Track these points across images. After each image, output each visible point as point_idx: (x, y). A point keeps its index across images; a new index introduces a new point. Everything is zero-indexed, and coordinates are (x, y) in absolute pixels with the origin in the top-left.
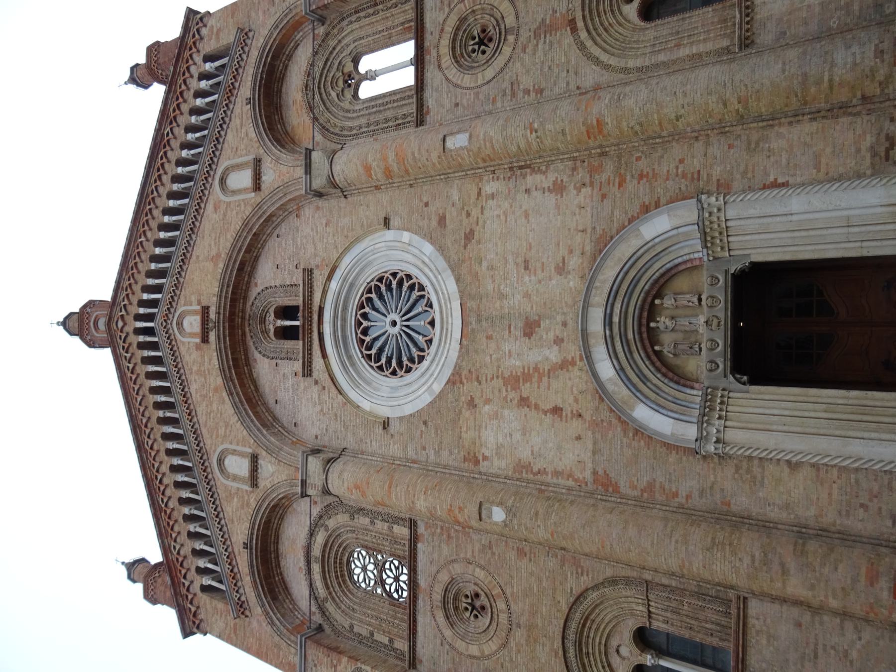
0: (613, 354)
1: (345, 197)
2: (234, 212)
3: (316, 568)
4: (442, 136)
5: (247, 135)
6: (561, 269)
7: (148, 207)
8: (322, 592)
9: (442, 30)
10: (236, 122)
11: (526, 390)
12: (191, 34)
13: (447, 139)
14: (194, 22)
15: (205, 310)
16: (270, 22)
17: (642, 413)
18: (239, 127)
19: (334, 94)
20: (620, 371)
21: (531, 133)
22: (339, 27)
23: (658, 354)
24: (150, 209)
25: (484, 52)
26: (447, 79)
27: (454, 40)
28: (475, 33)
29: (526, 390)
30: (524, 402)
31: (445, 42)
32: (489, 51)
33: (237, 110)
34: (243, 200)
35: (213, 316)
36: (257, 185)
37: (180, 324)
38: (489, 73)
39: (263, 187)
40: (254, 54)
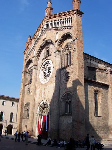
0: (42, 104)
3: (30, 69)
6: (48, 96)
8: (29, 71)
11: (40, 94)
15: (45, 39)
17: (39, 108)
20: (41, 105)
23: (44, 109)
29: (40, 94)
30: (40, 94)
35: (45, 40)
37: (45, 33)
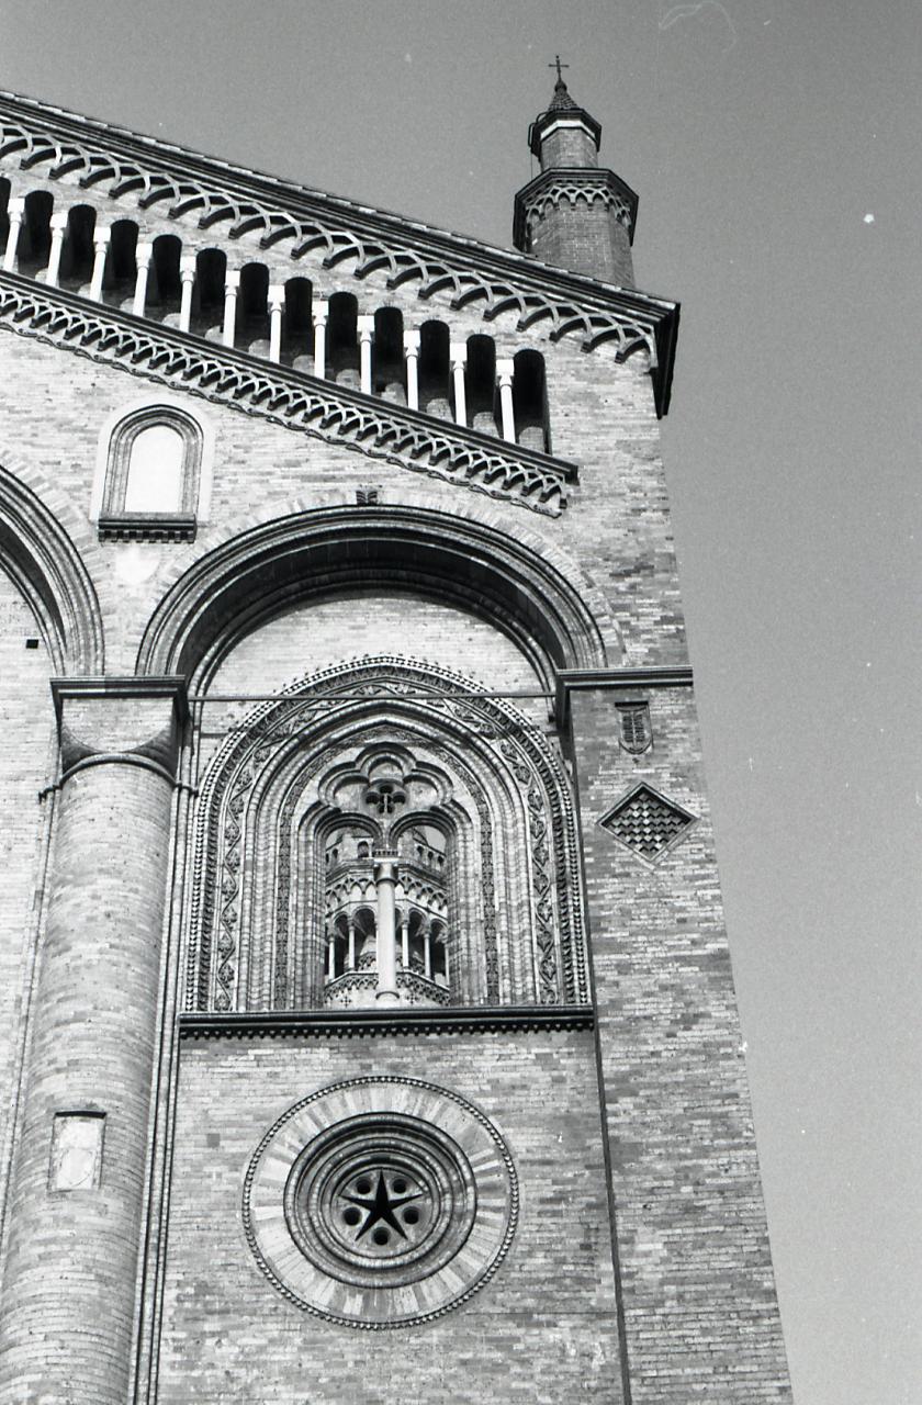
1: (42, 796)
2: (60, 455)
4: (101, 1104)
5: (272, 495)
7: (147, 176)
9: (436, 1090)
10: (319, 458)
12: (605, 314)
13: (95, 1125)
14: (636, 324)
16: (567, 566)
18: (304, 469)
19: (350, 755)
21: (30, 1385)
22: (533, 767)
24: (141, 184)
25: (351, 1218)
26: (295, 1108)
27: (402, 1128)
28: (413, 1191)
31: (399, 1100)
32: (347, 1233)
33: (353, 464)
34: (88, 484)
36: (116, 530)
38: (275, 1240)
39: (112, 547)
40: (490, 513)
